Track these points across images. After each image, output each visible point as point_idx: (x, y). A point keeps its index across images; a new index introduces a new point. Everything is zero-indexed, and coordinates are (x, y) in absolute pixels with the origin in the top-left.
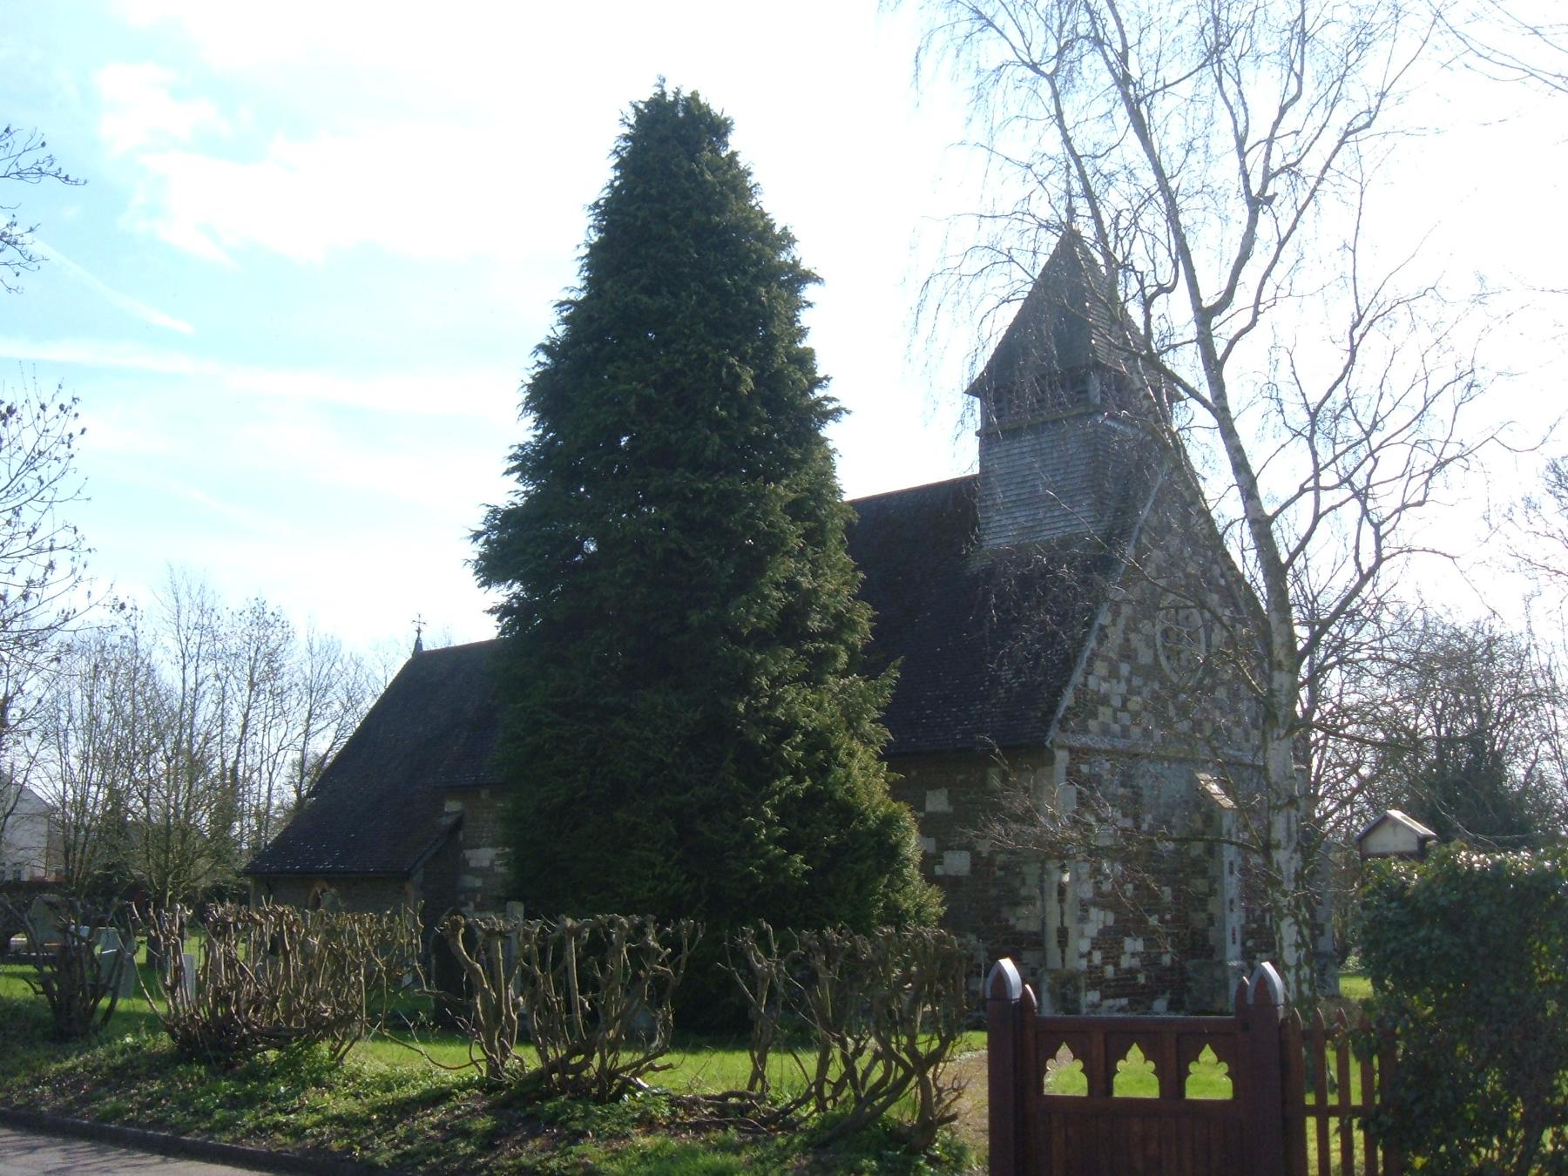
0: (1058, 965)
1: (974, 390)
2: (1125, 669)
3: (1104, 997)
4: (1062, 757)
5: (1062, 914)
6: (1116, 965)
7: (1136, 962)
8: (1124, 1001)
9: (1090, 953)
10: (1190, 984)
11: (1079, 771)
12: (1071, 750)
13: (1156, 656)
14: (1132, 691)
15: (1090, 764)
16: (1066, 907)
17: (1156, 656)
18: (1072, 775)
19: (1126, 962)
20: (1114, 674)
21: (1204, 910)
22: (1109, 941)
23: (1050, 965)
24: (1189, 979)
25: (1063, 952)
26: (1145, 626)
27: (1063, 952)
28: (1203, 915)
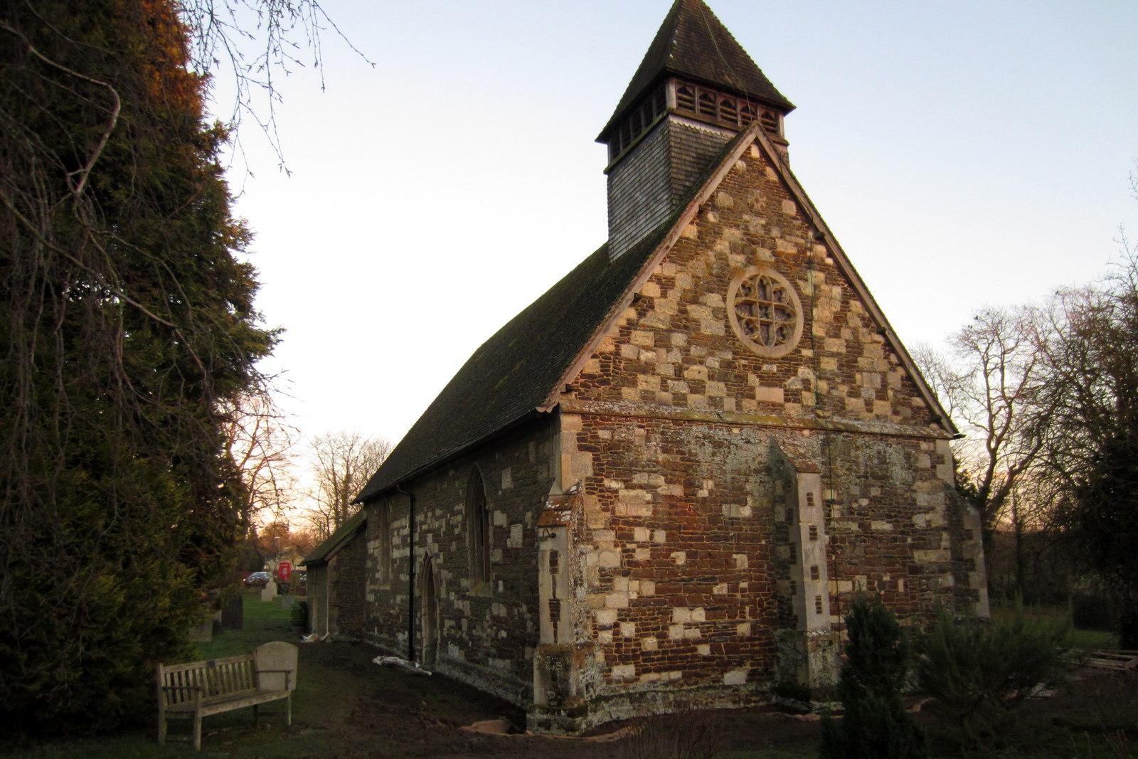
0: (551, 640)
1: (602, 138)
2: (679, 339)
3: (642, 671)
4: (570, 425)
5: (554, 583)
6: (662, 636)
7: (695, 633)
8: (676, 675)
9: (616, 625)
10: (779, 654)
11: (595, 437)
12: (584, 415)
13: (728, 327)
14: (688, 360)
15: (613, 430)
16: (557, 577)
17: (728, 327)
18: (584, 443)
19: (675, 633)
20: (662, 341)
21: (788, 578)
22: (649, 614)
23: (543, 640)
24: (777, 649)
25: (555, 626)
26: (714, 299)
27: (555, 626)
28: (787, 583)
